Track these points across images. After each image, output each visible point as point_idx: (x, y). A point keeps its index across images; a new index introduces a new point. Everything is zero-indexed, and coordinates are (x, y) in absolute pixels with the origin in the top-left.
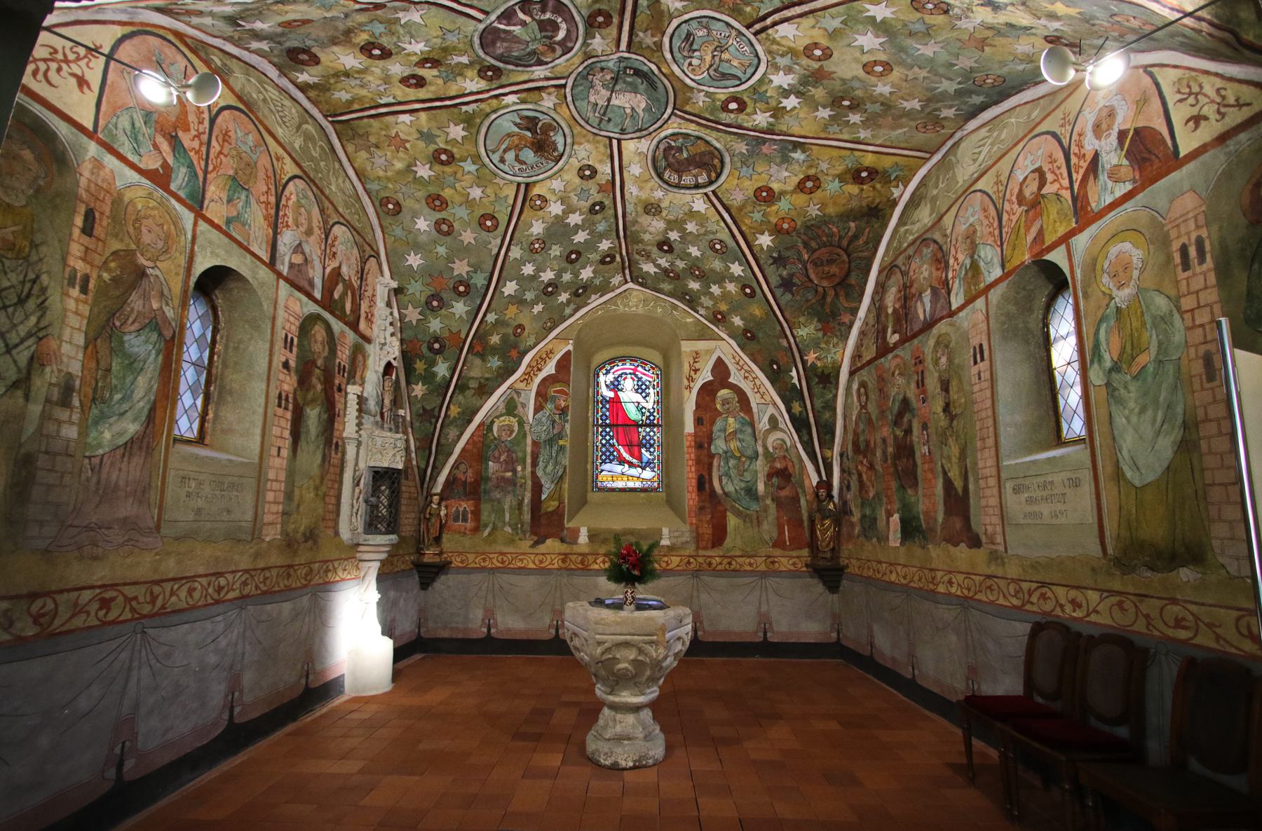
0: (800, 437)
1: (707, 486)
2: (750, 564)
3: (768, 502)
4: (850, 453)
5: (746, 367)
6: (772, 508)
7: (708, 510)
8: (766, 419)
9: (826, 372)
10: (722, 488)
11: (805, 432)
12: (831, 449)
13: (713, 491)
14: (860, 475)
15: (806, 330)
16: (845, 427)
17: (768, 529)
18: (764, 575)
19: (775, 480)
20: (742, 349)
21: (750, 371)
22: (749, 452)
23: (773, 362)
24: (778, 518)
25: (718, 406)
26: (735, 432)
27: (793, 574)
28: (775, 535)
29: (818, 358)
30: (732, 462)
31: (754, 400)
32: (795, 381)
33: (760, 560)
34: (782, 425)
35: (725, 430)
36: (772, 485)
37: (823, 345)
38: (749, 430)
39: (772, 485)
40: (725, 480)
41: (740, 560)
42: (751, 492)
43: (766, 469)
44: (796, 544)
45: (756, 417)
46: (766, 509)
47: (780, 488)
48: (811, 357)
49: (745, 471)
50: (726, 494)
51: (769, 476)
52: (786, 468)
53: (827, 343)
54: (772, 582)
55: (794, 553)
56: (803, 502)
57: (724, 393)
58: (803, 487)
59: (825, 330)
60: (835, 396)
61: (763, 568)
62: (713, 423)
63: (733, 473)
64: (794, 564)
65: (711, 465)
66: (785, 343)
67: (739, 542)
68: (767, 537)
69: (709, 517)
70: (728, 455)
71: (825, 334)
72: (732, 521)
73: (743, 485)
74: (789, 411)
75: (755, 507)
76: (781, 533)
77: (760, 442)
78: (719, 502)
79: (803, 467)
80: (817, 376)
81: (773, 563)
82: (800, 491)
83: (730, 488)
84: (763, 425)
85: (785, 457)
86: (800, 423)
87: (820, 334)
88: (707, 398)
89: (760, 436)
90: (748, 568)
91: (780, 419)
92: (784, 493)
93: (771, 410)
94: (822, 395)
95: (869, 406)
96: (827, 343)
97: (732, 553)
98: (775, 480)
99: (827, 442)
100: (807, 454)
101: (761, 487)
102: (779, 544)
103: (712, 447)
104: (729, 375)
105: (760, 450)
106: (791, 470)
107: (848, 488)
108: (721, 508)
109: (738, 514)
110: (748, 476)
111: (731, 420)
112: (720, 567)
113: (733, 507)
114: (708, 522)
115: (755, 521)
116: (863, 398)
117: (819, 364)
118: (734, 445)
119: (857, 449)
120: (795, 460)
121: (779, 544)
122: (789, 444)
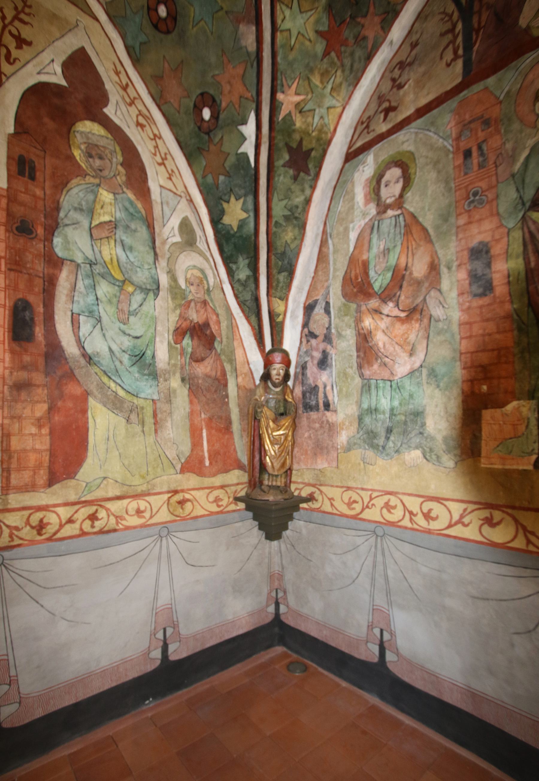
0: (230, 273)
1: (39, 331)
2: (139, 512)
3: (175, 383)
4: (336, 298)
5: (141, 107)
6: (182, 394)
7: (41, 393)
8: (175, 222)
9: (306, 145)
10: (81, 347)
11: (243, 262)
12: (285, 298)
13: (54, 351)
14: (364, 341)
15: (300, 20)
16: (322, 257)
17: (176, 436)
18: (165, 530)
19: (187, 341)
20: (136, 61)
21: (150, 119)
22: (141, 277)
23: (207, 99)
24: (192, 413)
25: (77, 154)
26: (113, 225)
27: (217, 519)
28: (186, 448)
29: (300, 108)
30: (104, 289)
31: (156, 180)
32: (248, 148)
33: (157, 501)
34: (201, 244)
35: (91, 212)
36: (183, 352)
37: (316, 80)
38: (143, 232)
39: (183, 352)
40: (85, 327)
41: (115, 507)
42: (142, 360)
43: (174, 318)
44: (224, 461)
45: (157, 211)
46: (169, 397)
47: (197, 359)
48: (288, 100)
49: (135, 313)
50: (89, 358)
51: (179, 333)
52: (207, 325)
53: (325, 75)
54: (181, 541)
55: (218, 480)
56: (232, 390)
57: (87, 128)
58: (232, 361)
59: (332, 39)
60: (308, 201)
61: (164, 516)
62: (61, 185)
63: (107, 312)
64: (217, 500)
65: (50, 284)
66: (249, 41)
67: (115, 469)
68: (171, 454)
69: (41, 409)
70: (95, 269)
71: (326, 53)
72: (101, 422)
73: (127, 342)
74: (215, 222)
75: (148, 390)
76: (196, 443)
77: (163, 263)
78: (71, 375)
79: (233, 327)
80: (290, 150)
81: (182, 503)
82: (228, 367)
83: (96, 344)
84: (170, 231)
85: (205, 303)
86: (235, 246)
87: (320, 47)
88: (50, 124)
89: (164, 250)
90: (134, 521)
91: (199, 232)
92: (202, 369)
93: (183, 210)
94: (288, 194)
95: (413, 202)
96: (325, 75)
97: (99, 494)
98: (187, 341)
99: (280, 287)
100: (241, 304)
101: (162, 353)
102: (192, 466)
103: (57, 241)
104: (104, 99)
105: (164, 280)
106: (214, 327)
107: (324, 363)
108: (72, 389)
109: (115, 404)
110: (137, 326)
111: (106, 196)
112: (69, 530)
113: (102, 387)
114: (39, 423)
115: (149, 420)
116: (390, 192)
117: (299, 123)
118: (109, 251)
119: (358, 287)
120: (221, 311)
121: (192, 466)
122: (211, 281)
